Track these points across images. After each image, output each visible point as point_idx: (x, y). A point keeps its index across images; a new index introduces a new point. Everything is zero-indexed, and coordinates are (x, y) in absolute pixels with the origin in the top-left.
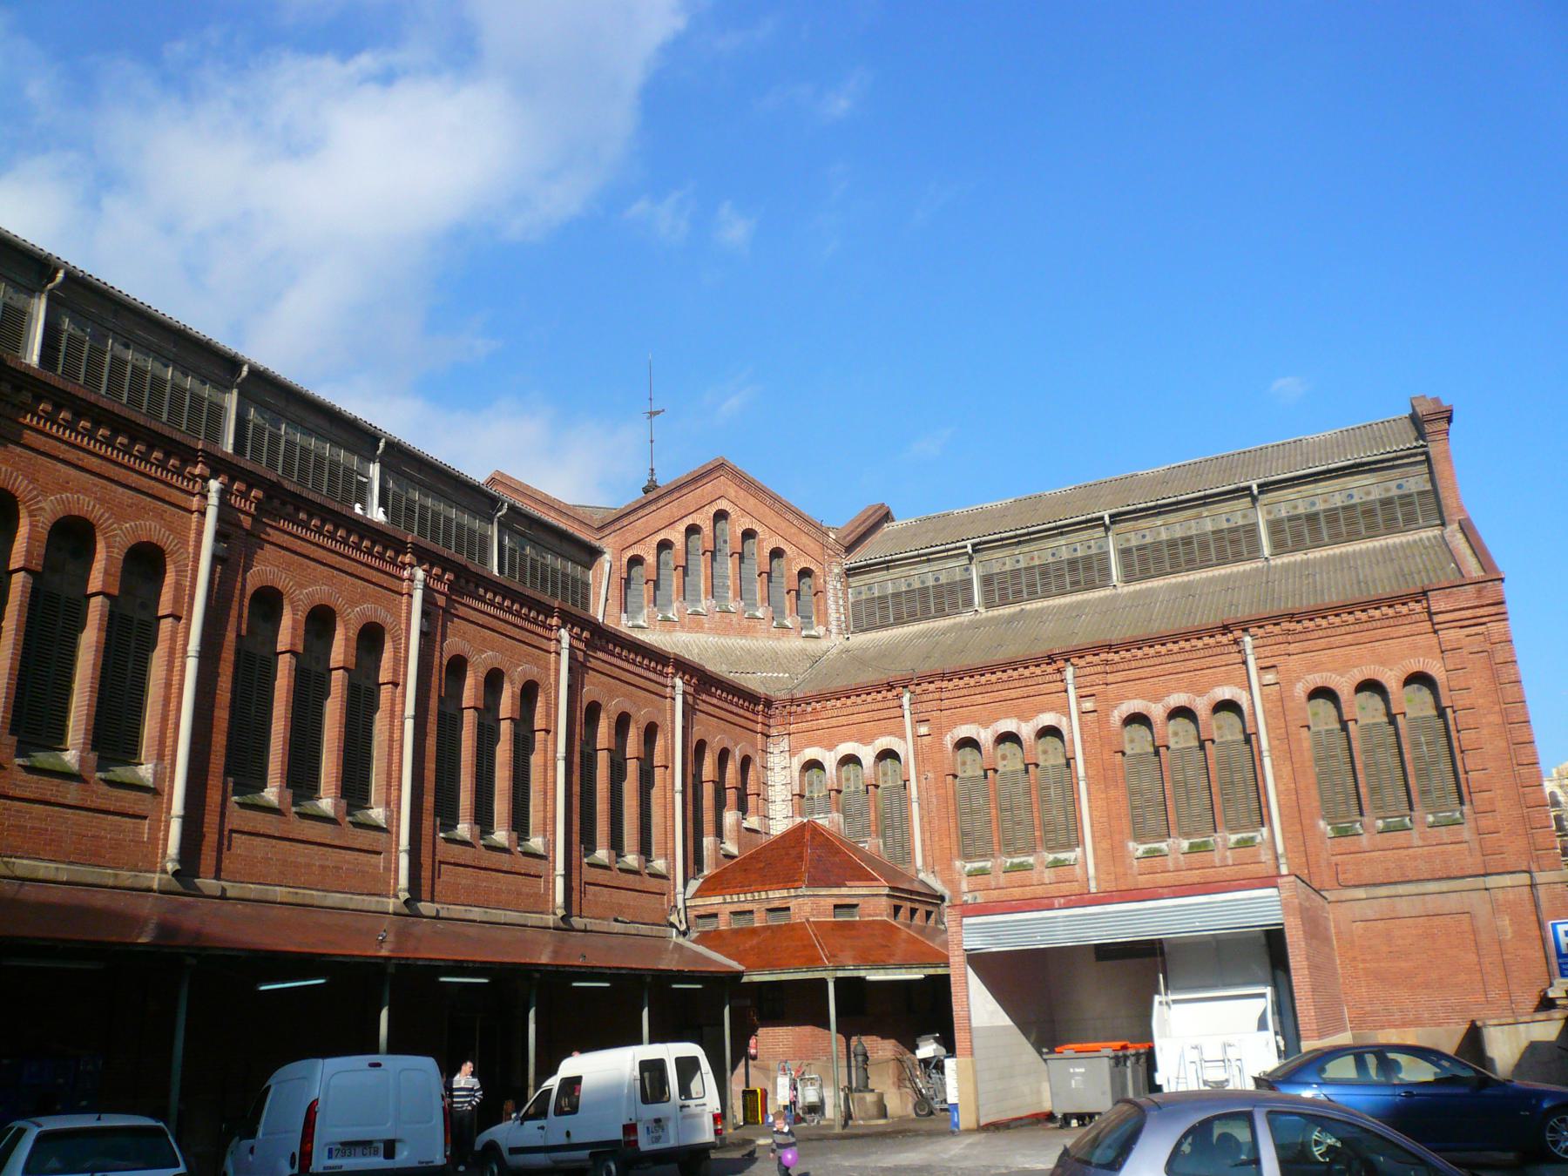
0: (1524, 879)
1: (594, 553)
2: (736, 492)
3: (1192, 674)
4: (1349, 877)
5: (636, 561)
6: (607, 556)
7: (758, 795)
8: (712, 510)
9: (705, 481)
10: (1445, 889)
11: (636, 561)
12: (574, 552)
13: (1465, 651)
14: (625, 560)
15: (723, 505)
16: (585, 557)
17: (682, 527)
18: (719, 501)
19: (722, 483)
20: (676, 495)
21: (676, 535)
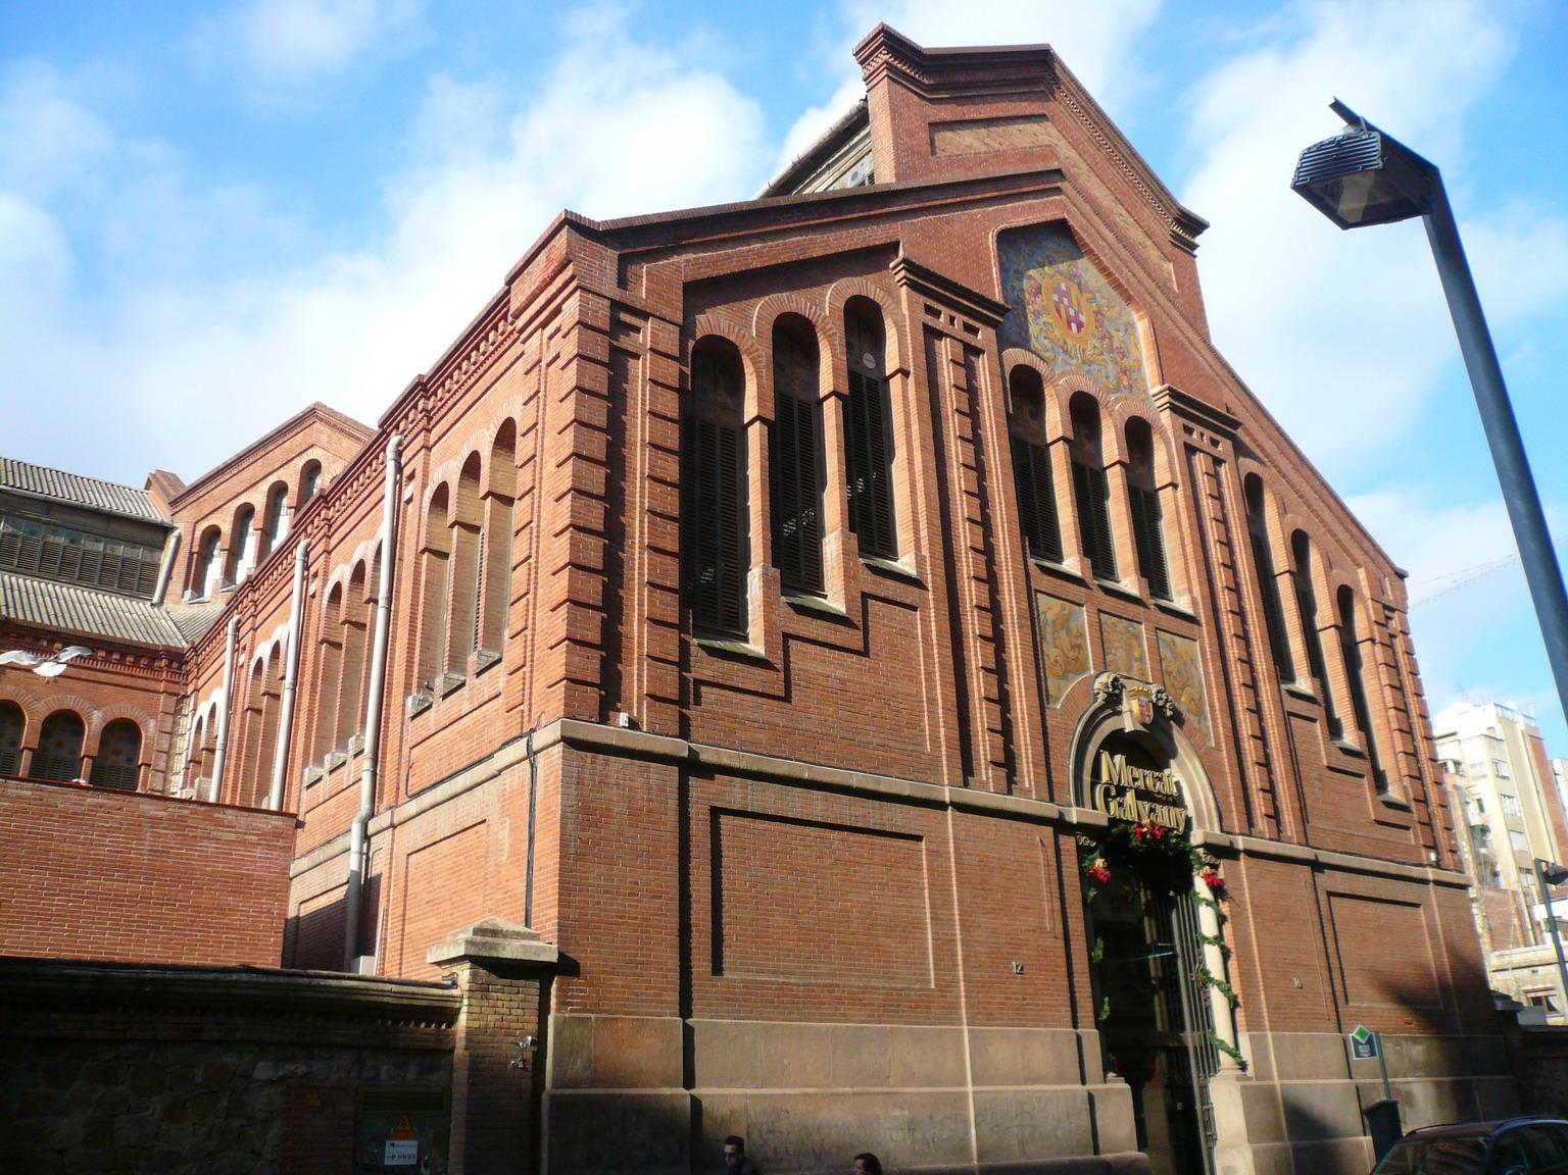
0: (519, 749)
1: (165, 530)
2: (329, 437)
3: (374, 510)
4: (416, 784)
5: (213, 534)
6: (176, 533)
7: (149, 765)
8: (300, 462)
9: (294, 433)
10: (469, 784)
11: (213, 534)
12: (138, 534)
13: (543, 364)
14: (198, 533)
15: (314, 454)
16: (159, 537)
17: (265, 487)
18: (310, 450)
19: (319, 432)
20: (262, 453)
21: (258, 498)
